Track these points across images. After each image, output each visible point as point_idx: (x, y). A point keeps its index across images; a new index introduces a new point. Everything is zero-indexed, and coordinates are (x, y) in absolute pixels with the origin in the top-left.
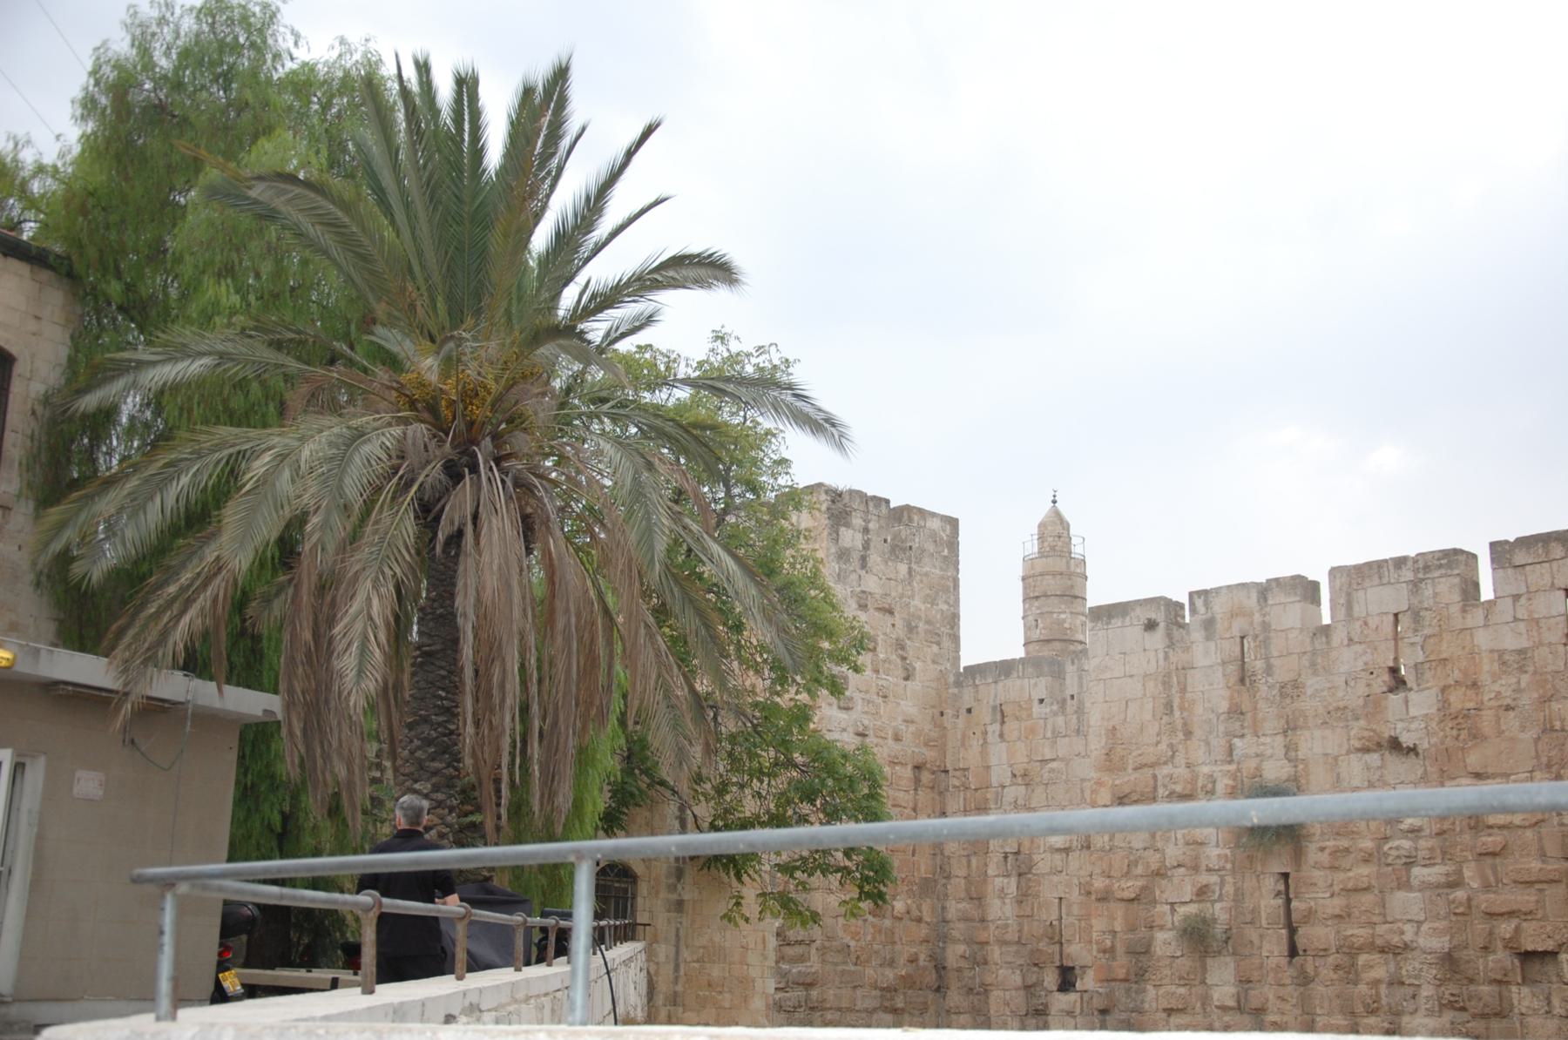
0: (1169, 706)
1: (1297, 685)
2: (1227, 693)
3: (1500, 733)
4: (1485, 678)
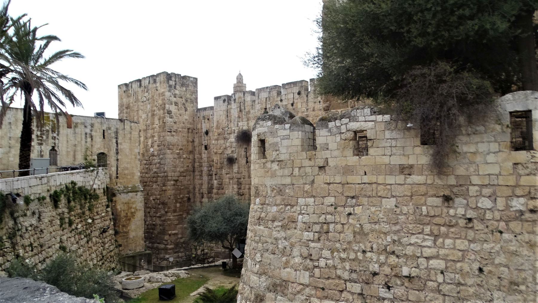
0: (227, 116)
1: (249, 111)
2: (237, 114)
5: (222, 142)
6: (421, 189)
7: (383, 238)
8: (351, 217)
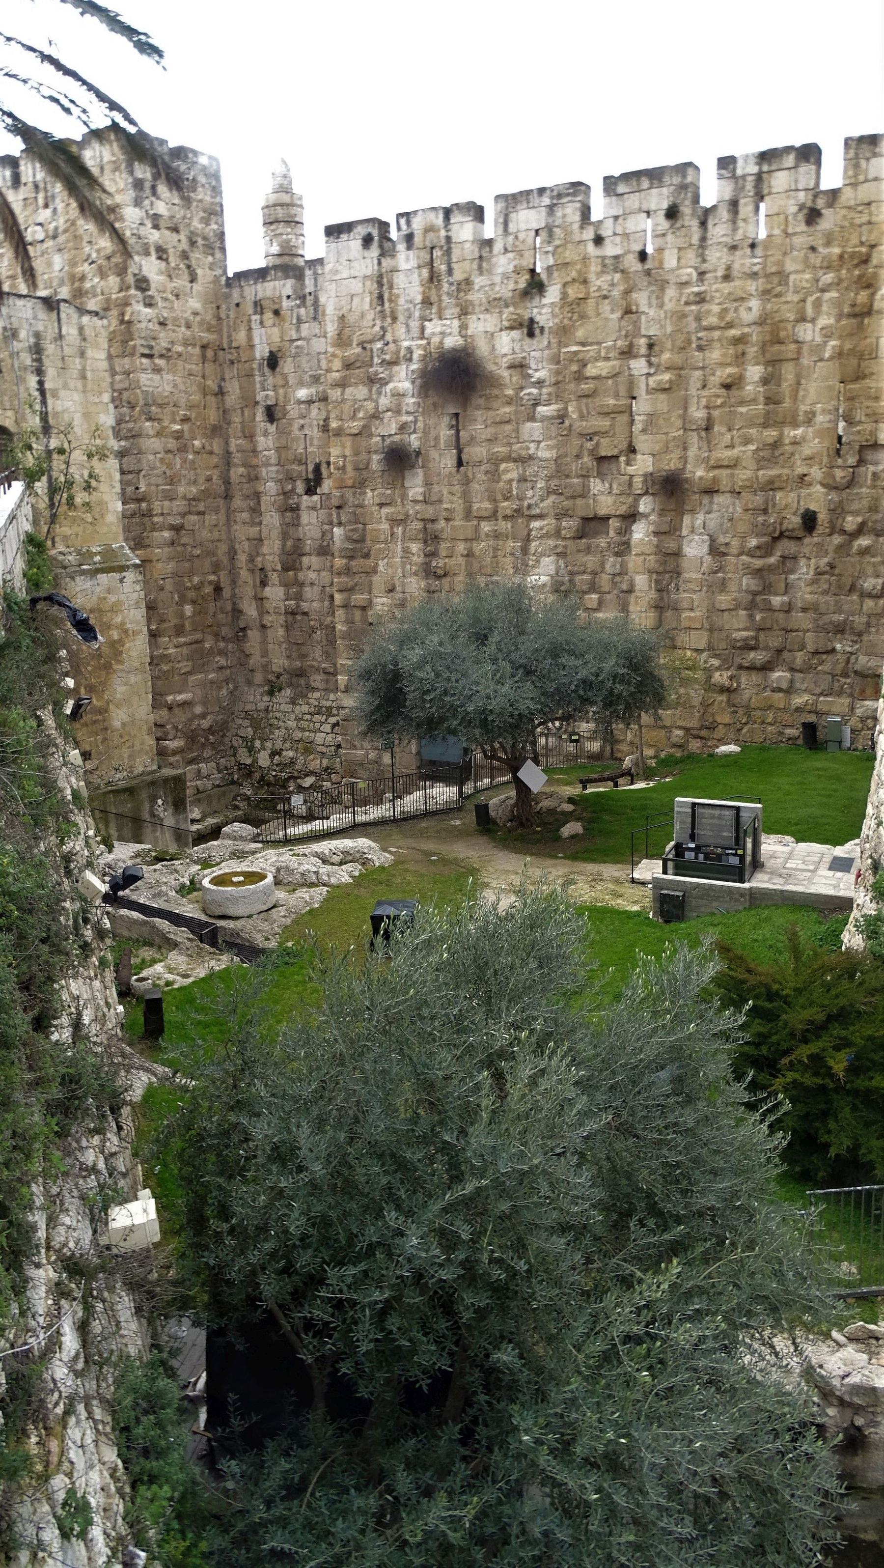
0: (381, 297)
1: (468, 282)
2: (421, 289)
3: (598, 314)
4: (592, 277)
5: (361, 392)
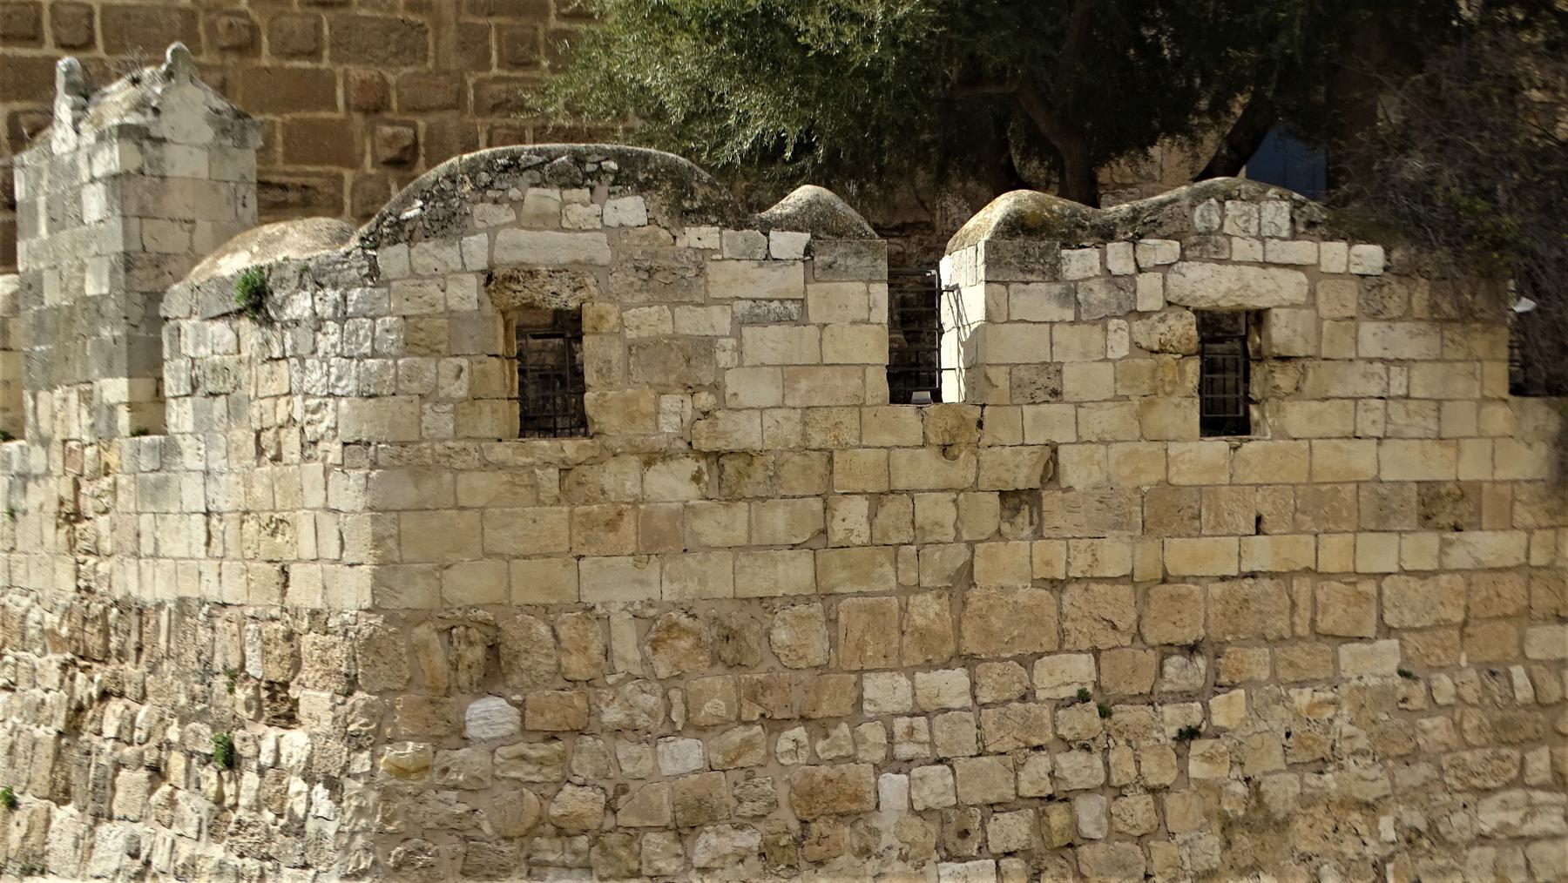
6: (1506, 591)
7: (1362, 829)
8: (1198, 747)
